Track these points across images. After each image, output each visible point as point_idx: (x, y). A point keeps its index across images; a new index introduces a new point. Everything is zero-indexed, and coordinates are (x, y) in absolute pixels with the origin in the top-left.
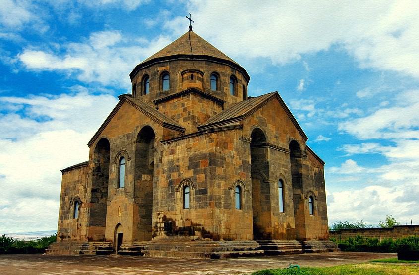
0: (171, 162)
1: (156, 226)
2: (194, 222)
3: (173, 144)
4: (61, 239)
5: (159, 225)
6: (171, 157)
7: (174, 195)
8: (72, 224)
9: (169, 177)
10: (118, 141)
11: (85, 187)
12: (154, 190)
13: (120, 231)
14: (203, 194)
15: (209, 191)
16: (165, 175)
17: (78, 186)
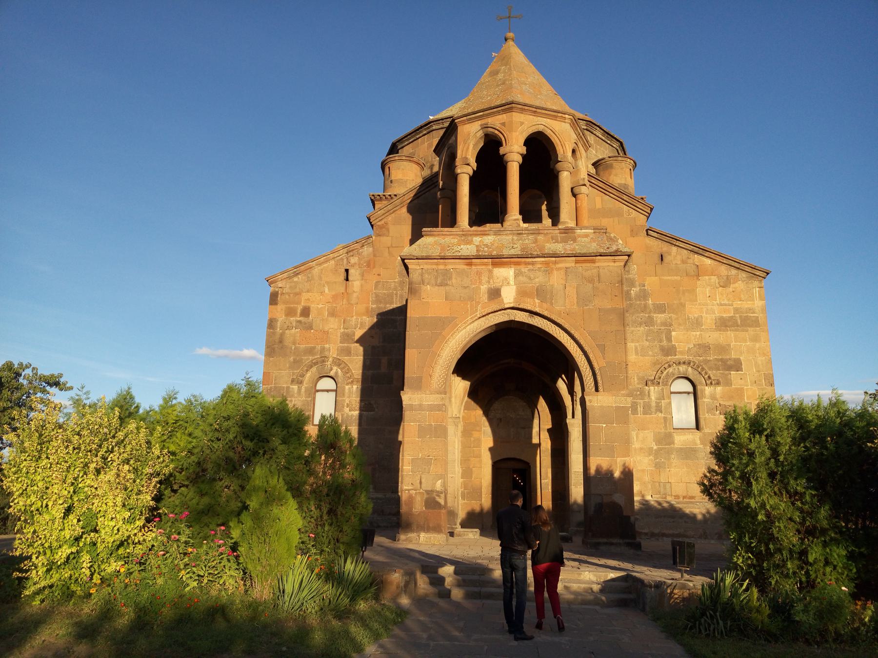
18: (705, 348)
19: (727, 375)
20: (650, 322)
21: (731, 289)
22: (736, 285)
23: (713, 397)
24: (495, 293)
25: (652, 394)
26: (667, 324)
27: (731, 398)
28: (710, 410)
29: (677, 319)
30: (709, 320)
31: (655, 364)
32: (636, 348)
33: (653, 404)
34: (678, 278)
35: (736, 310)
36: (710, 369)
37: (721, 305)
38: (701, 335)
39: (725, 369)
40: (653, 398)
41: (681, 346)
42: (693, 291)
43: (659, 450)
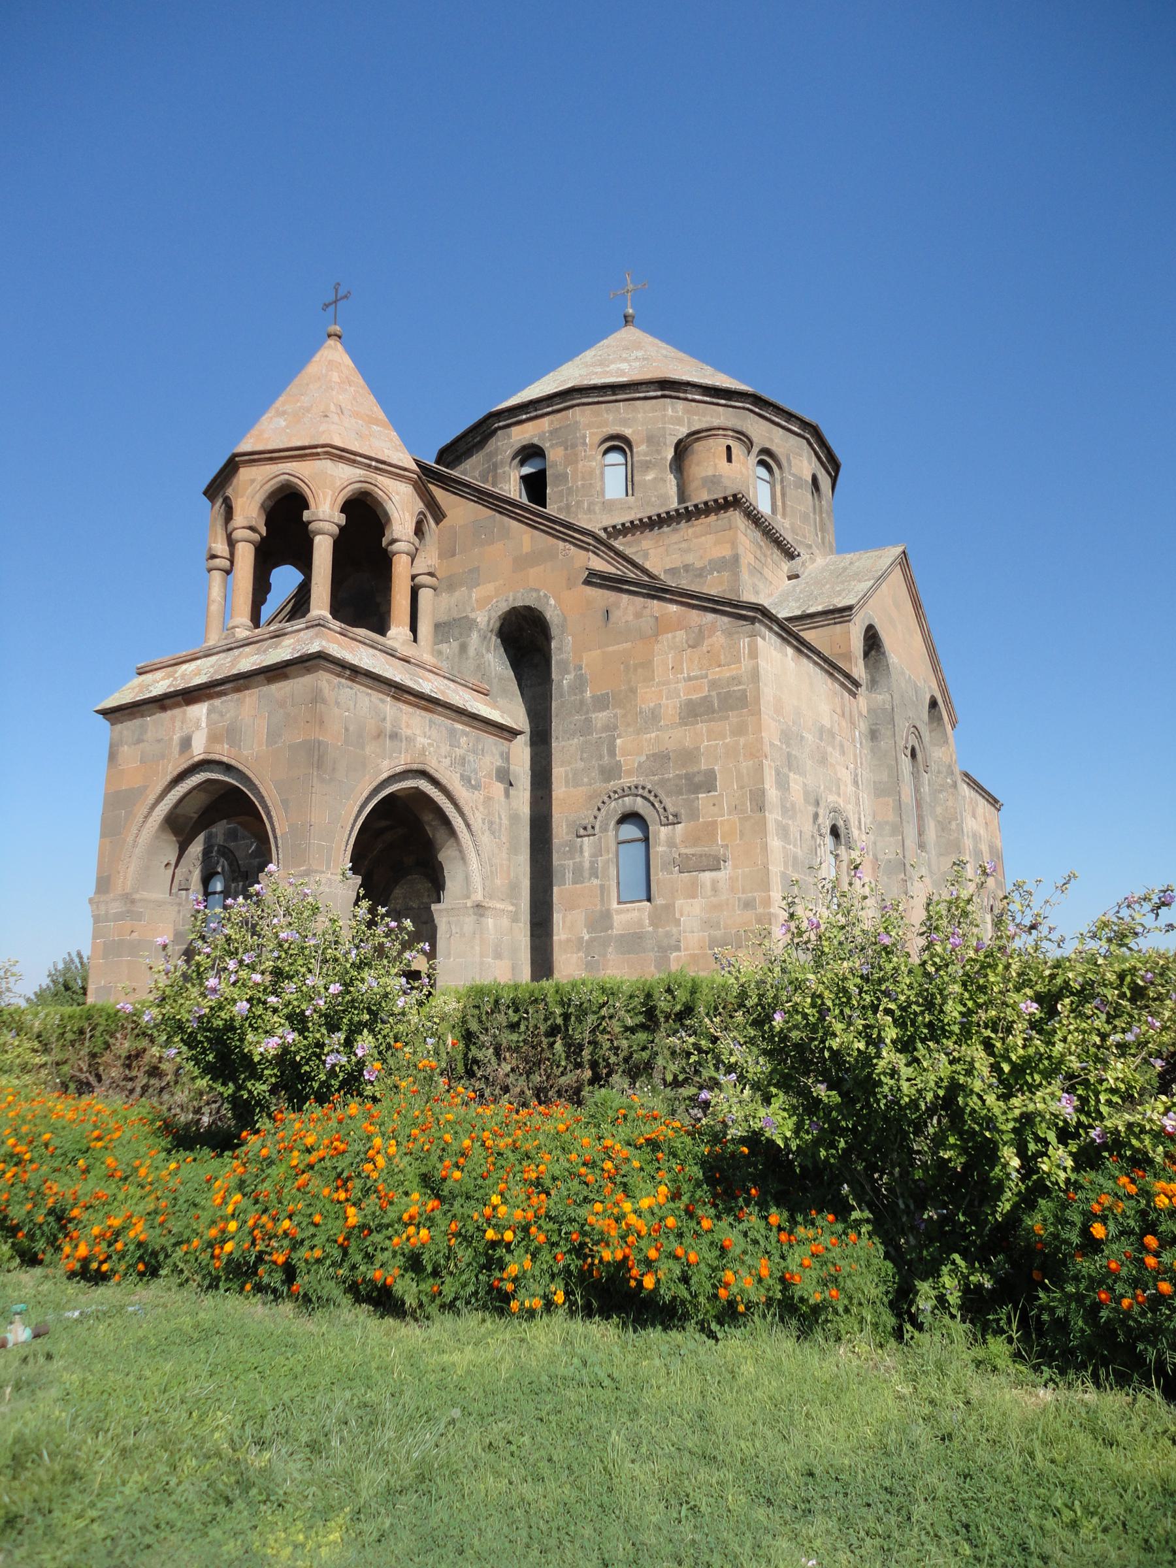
11: (856, 783)
17: (834, 755)
18: (661, 759)
19: (693, 801)
20: (586, 728)
21: (705, 649)
22: (714, 639)
23: (671, 844)
24: (186, 743)
25: (586, 848)
26: (611, 728)
27: (695, 840)
28: (665, 867)
29: (624, 716)
30: (671, 707)
31: (590, 798)
32: (567, 776)
33: (587, 865)
34: (628, 645)
35: (713, 684)
36: (668, 794)
37: (690, 679)
38: (657, 736)
39: (690, 792)
40: (586, 854)
42: (647, 665)
43: (592, 940)
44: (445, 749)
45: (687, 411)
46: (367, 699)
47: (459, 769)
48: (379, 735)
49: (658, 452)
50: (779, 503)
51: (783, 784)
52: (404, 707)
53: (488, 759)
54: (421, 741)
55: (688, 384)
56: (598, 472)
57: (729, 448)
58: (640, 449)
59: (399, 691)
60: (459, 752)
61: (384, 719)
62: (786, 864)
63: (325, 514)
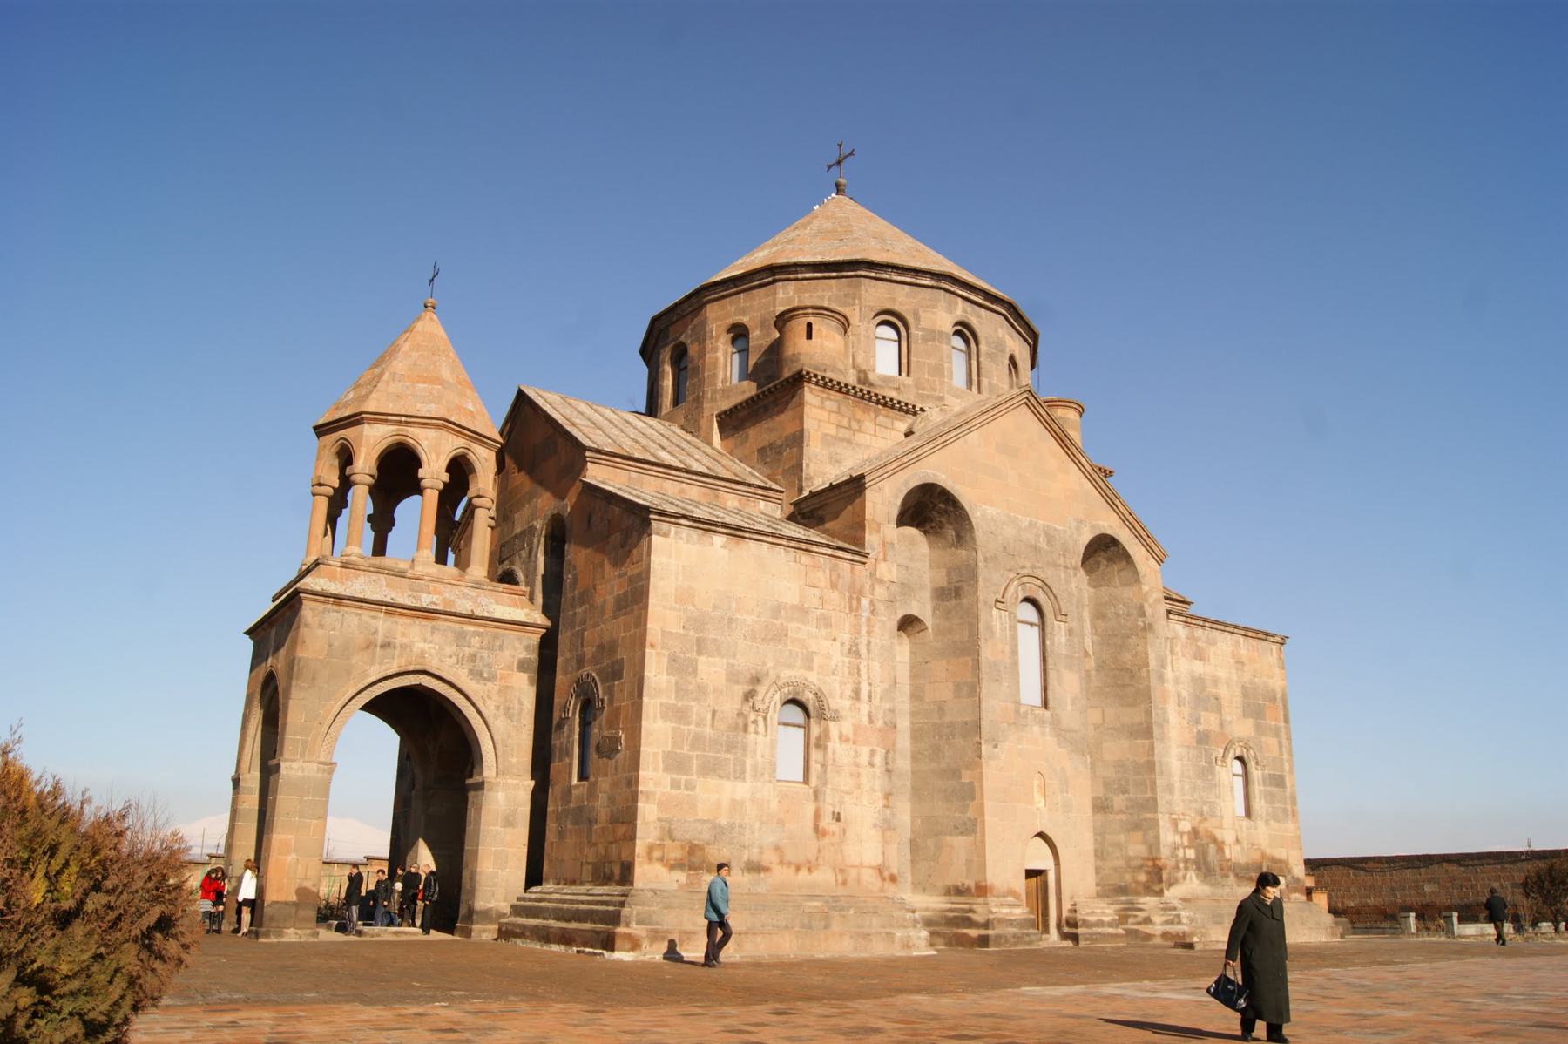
0: (1198, 682)
1: (1174, 855)
2: (1269, 851)
3: (1199, 632)
4: (681, 876)
5: (1181, 853)
6: (1198, 667)
7: (1213, 773)
8: (774, 805)
9: (1197, 722)
10: (1009, 532)
11: (854, 652)
12: (1158, 747)
13: (1043, 860)
14: (1278, 785)
15: (1288, 784)
16: (1186, 711)
41: (589, 651)
44: (450, 649)
45: (798, 291)
46: (356, 619)
47: (468, 666)
48: (369, 646)
49: (769, 335)
50: (904, 361)
51: (681, 667)
52: (401, 620)
53: (507, 653)
54: (419, 645)
55: (796, 265)
56: (722, 360)
57: (809, 325)
58: (755, 334)
59: (392, 608)
60: (467, 650)
61: (376, 632)
62: (674, 744)
63: (365, 466)
